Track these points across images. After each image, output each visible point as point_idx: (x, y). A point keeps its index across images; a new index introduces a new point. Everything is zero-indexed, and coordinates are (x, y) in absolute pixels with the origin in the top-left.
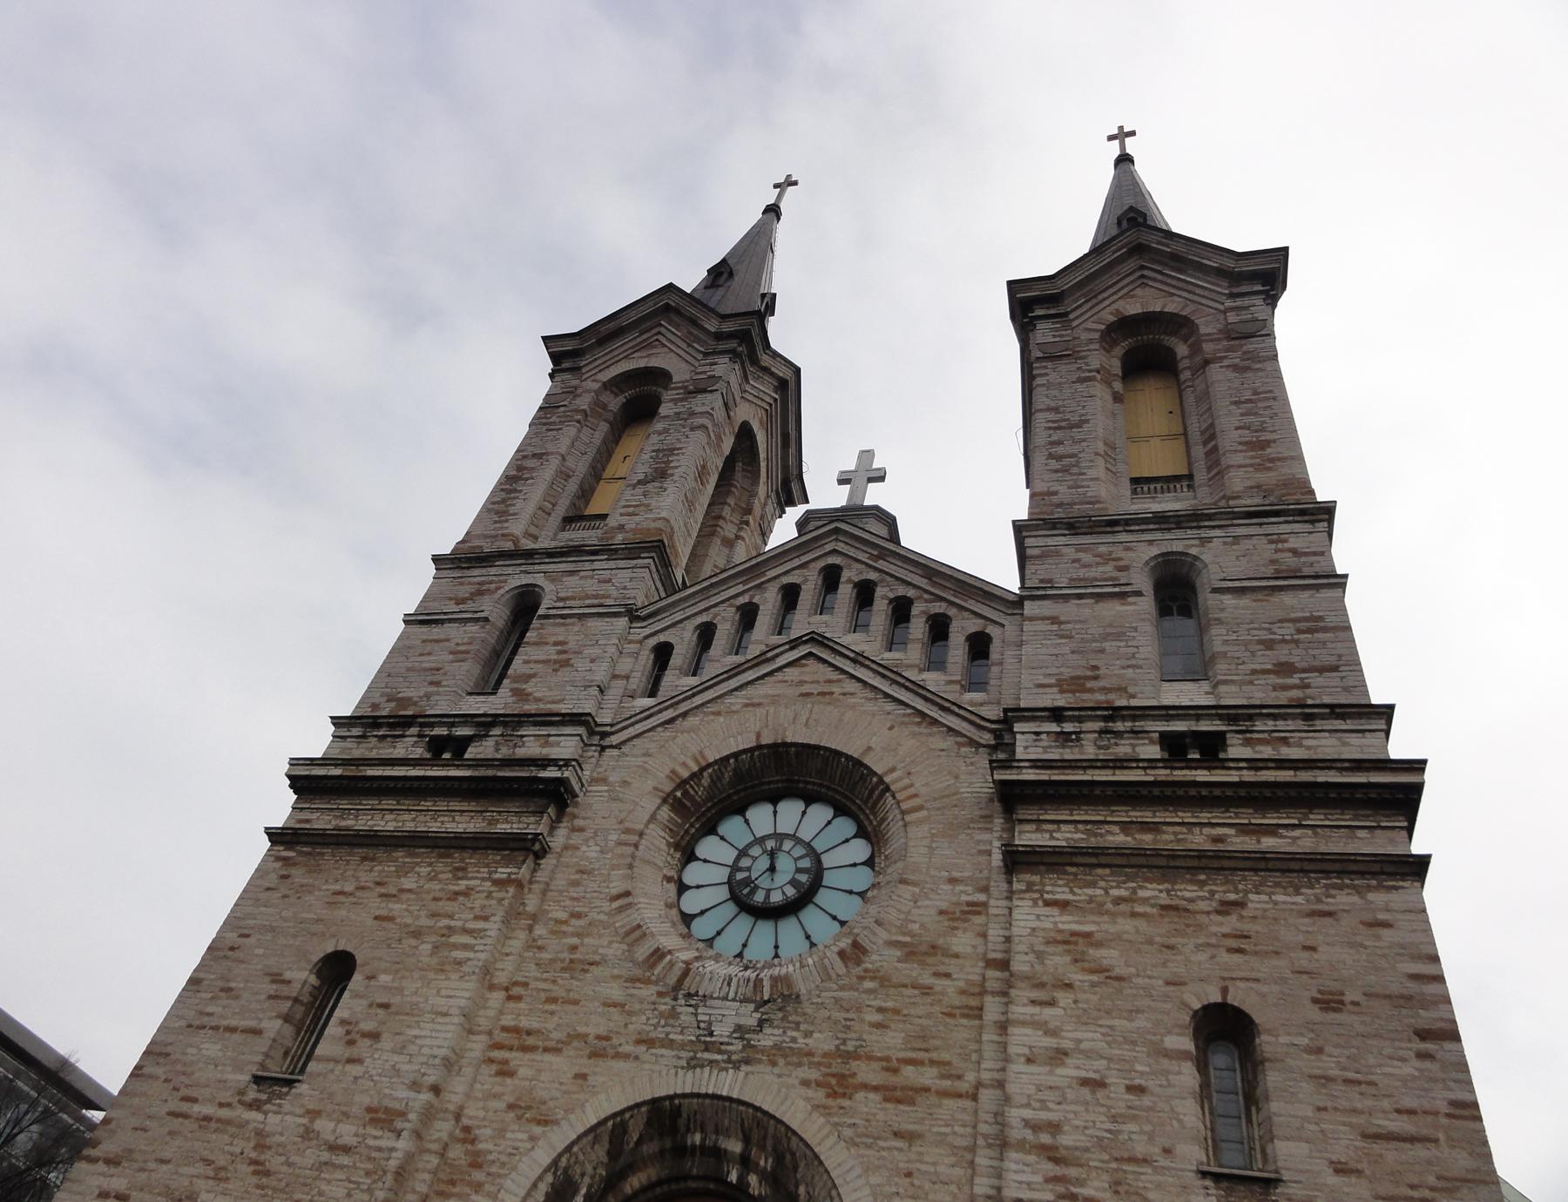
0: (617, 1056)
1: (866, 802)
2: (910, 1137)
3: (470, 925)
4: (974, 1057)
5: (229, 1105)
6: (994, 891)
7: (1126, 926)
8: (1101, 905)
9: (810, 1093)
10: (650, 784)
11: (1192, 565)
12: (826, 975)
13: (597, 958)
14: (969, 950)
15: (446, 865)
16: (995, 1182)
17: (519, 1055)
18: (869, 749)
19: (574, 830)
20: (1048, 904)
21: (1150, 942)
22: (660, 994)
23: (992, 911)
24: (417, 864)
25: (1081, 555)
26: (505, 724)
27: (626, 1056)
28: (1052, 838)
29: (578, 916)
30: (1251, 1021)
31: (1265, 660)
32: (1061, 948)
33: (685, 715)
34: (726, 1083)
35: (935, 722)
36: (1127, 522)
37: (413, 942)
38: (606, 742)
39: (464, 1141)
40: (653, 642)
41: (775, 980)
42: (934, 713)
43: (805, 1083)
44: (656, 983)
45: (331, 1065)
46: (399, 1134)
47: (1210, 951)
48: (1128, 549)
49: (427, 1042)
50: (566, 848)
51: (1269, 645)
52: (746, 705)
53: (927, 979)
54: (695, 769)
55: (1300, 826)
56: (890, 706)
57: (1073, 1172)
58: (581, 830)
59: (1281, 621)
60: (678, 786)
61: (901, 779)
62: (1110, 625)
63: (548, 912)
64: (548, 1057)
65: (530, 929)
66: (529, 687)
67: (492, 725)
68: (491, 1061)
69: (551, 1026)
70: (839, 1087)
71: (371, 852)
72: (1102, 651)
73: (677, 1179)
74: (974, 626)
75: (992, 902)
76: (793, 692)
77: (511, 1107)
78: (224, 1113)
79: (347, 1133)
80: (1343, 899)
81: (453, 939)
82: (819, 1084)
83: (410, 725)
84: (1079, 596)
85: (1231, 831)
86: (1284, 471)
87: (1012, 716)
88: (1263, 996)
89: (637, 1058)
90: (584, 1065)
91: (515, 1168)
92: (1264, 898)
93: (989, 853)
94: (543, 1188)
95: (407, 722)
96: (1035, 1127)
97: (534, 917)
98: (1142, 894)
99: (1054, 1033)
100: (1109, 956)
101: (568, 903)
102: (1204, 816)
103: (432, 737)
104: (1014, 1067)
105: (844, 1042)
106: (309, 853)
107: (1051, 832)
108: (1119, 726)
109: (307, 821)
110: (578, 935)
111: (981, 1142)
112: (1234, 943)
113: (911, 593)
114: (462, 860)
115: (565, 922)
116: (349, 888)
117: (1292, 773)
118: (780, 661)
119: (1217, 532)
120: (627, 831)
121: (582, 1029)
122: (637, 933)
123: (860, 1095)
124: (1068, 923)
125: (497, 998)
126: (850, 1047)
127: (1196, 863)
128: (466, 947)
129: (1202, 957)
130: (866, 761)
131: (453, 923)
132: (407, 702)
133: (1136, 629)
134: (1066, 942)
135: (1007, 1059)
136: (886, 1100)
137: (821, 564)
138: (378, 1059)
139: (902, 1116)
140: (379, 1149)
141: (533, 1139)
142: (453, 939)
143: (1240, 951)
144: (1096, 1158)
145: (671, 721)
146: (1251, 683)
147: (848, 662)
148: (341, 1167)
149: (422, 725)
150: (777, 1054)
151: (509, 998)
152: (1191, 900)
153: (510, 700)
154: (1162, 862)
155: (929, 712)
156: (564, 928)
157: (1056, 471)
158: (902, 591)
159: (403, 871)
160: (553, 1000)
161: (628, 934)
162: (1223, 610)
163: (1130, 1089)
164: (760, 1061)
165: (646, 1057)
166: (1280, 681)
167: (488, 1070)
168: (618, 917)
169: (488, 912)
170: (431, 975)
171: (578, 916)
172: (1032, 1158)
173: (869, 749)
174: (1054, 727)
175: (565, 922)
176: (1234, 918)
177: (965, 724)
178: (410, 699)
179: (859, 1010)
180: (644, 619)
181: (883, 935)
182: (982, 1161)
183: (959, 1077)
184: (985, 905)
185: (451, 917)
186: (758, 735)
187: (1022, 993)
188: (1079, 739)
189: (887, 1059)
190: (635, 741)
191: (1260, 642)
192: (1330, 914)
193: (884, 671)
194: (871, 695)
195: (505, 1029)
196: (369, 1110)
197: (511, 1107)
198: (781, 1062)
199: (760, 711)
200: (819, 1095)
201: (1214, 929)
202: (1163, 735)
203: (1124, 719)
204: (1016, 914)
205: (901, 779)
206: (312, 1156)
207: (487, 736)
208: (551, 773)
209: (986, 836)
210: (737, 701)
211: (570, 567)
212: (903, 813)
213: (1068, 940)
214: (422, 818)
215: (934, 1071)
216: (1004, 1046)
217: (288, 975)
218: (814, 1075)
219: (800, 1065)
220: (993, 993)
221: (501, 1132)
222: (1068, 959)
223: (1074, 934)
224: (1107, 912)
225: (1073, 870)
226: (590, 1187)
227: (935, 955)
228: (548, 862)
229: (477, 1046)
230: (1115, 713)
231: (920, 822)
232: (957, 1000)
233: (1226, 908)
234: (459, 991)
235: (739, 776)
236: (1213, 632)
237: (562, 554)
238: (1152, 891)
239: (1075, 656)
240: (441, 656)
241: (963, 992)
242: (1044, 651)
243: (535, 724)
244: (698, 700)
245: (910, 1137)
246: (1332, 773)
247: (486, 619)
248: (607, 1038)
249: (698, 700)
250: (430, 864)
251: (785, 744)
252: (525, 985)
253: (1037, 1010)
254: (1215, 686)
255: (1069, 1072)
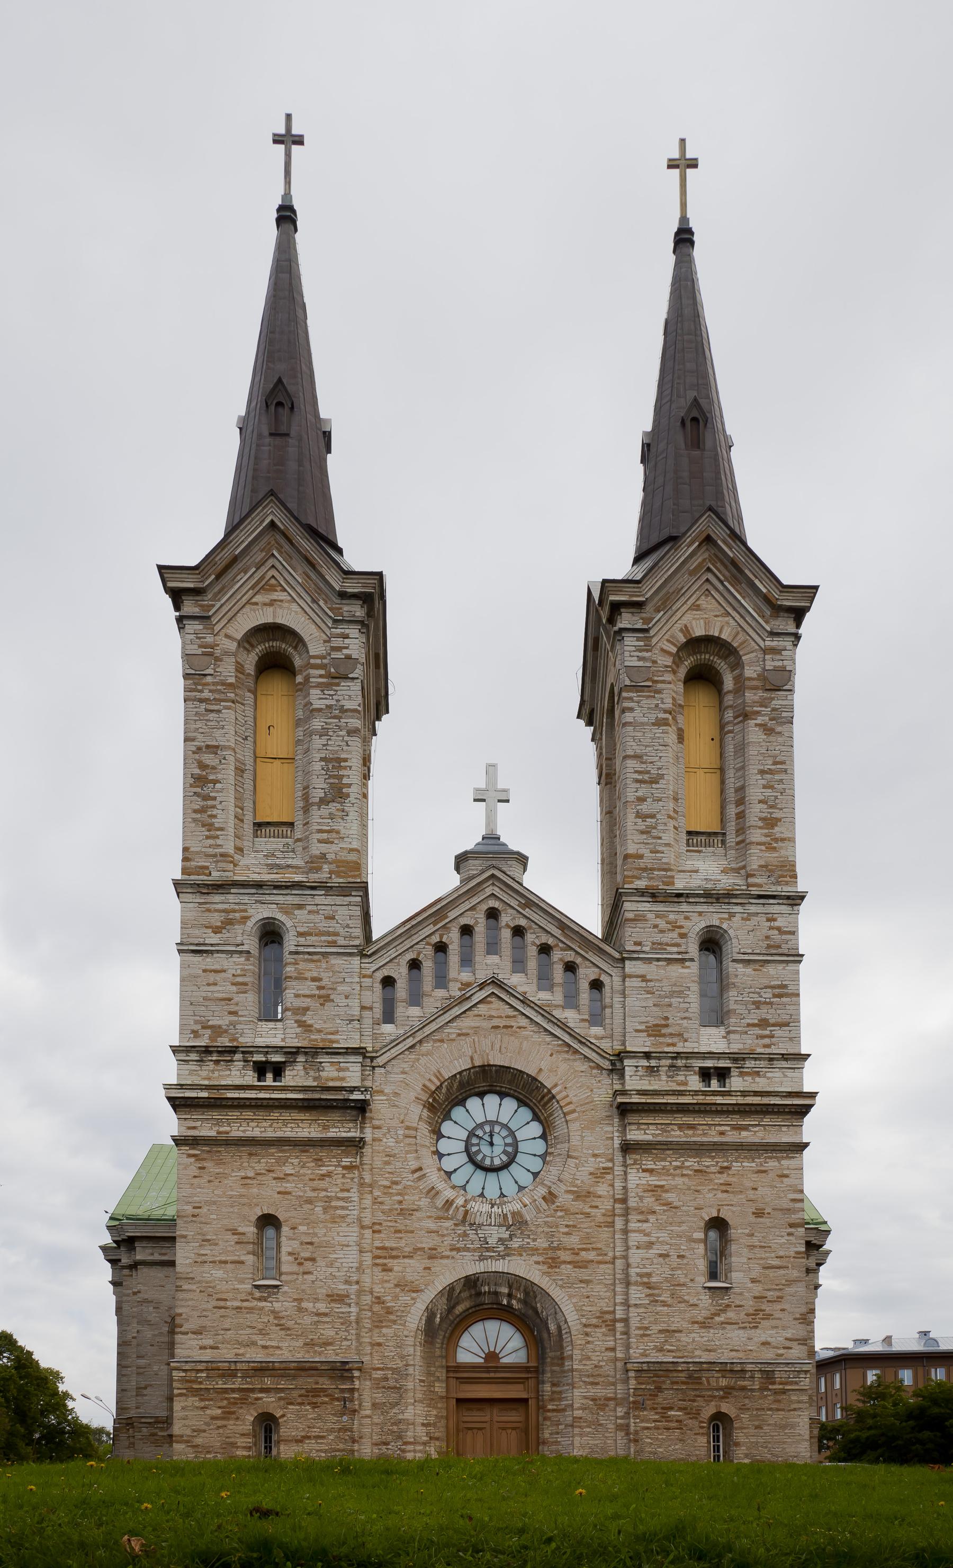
0: (442, 1257)
1: (539, 1102)
2: (587, 1282)
3: (340, 1195)
4: (612, 1245)
5: (247, 1300)
6: (617, 1163)
7: (679, 1181)
8: (668, 1170)
9: (540, 1267)
10: (412, 1095)
11: (722, 935)
12: (538, 1210)
13: (415, 1207)
14: (606, 1193)
15: (308, 1157)
16: (624, 1297)
17: (391, 1260)
18: (541, 1070)
19: (374, 1128)
20: (644, 1171)
21: (689, 1189)
22: (455, 1225)
23: (616, 1173)
24: (288, 1157)
25: (658, 921)
26: (306, 1053)
27: (448, 1257)
28: (645, 1133)
29: (396, 1183)
30: (728, 1223)
31: (753, 1018)
32: (651, 1193)
33: (420, 1042)
34: (500, 1266)
35: (576, 1052)
36: (688, 895)
37: (309, 1206)
38: (373, 1064)
39: (379, 1303)
40: (379, 975)
41: (514, 1214)
42: (576, 1046)
43: (537, 1263)
44: (451, 1219)
45: (295, 1276)
46: (350, 1305)
47: (715, 1192)
48: (687, 918)
49: (344, 1260)
50: (373, 1140)
51: (758, 1005)
52: (459, 1035)
53: (589, 1210)
54: (439, 1084)
55: (759, 1125)
56: (549, 1039)
57: (656, 1292)
58: (379, 1128)
59: (766, 987)
60: (431, 1096)
61: (560, 1092)
62: (675, 985)
63: (377, 1181)
64: (406, 1261)
65: (371, 1192)
66: (308, 1018)
67: (297, 1053)
68: (377, 1265)
69: (402, 1244)
70: (553, 1263)
71: (253, 1149)
72: (670, 1005)
73: (478, 1305)
74: (592, 974)
75: (616, 1168)
76: (487, 1024)
77: (396, 1286)
78: (245, 1304)
79: (322, 1307)
80: (772, 1164)
81: (333, 1204)
82: (544, 1263)
83: (234, 1052)
84: (658, 960)
85: (728, 1128)
86: (783, 852)
87: (621, 1056)
88: (733, 1212)
89: (453, 1258)
90: (427, 1263)
91: (409, 1312)
92: (739, 1164)
93: (612, 1138)
94: (424, 1318)
95: (233, 1051)
96: (641, 1275)
97: (371, 1186)
98: (687, 1164)
99: (646, 1235)
100: (671, 1197)
101: (387, 1175)
102: (717, 1120)
103: (254, 1062)
104: (631, 1251)
105: (552, 1242)
106: (209, 1152)
107: (645, 1130)
108: (680, 1063)
109: (194, 1128)
110: (400, 1194)
111: (617, 1282)
112: (724, 1188)
113: (551, 941)
114: (317, 1154)
115: (390, 1187)
116: (251, 1174)
117: (759, 1098)
118: (476, 999)
119: (738, 909)
120: (408, 1128)
121: (419, 1245)
122: (433, 1192)
123: (563, 1266)
124: (654, 1180)
125: (368, 1233)
126: (555, 1244)
127: (711, 1147)
128: (343, 1208)
129: (711, 1195)
131: (329, 1194)
132: (217, 1031)
133: (689, 988)
134: (653, 1191)
135: (628, 1248)
136: (575, 1267)
137: (484, 907)
138: (321, 1271)
139: (584, 1274)
140: (343, 1313)
141: (413, 1299)
142: (333, 1204)
143: (727, 1191)
144: (665, 1285)
145: (413, 1047)
146: (746, 1033)
147: (519, 1002)
148: (327, 1322)
149: (243, 1052)
150: (521, 1250)
151: (374, 1232)
152: (708, 1167)
153: (299, 1030)
154: (697, 1147)
155: (573, 1044)
156: (391, 1191)
157: (642, 832)
158: (545, 939)
159: (282, 1162)
160: (400, 1231)
162: (736, 976)
163: (679, 1257)
164: (514, 1255)
165: (458, 1256)
166: (760, 1032)
167: (376, 1269)
168: (420, 1183)
169: (347, 1187)
170: (330, 1225)
171: (396, 1183)
172: (640, 1288)
173: (541, 1070)
174: (644, 1063)
175: (390, 1187)
176: (725, 1175)
177: (594, 1054)
178: (220, 1027)
179: (557, 1226)
180: (370, 956)
181: (564, 1188)
182: (619, 1289)
183: (606, 1255)
184: (612, 1169)
185: (326, 1190)
186: (472, 1059)
187: (633, 1217)
188: (658, 1071)
189: (573, 1249)
190: (393, 1062)
191: (754, 1003)
192: (765, 1172)
193: (540, 1009)
194: (535, 1029)
195: (378, 1248)
196: (328, 1296)
197: (396, 1286)
198: (524, 1254)
199: (468, 1039)
200: (544, 1268)
201: (716, 1181)
202: (700, 1068)
203: (682, 1058)
204: (629, 1177)
205: (560, 1092)
206: (308, 1320)
207: (295, 1062)
208: (356, 1096)
209: (610, 1129)
210: (452, 1030)
211: (296, 900)
212: (565, 1114)
213: (655, 1190)
214: (275, 1125)
215: (594, 1253)
216: (626, 1240)
217: (241, 1230)
218: (541, 1259)
219: (533, 1255)
220: (619, 1216)
221: (396, 1298)
222: (653, 1199)
223: (656, 1186)
224: (671, 1175)
225: (655, 1151)
226: (441, 1314)
227: (589, 1197)
228: (367, 1150)
229: (368, 1259)
230: (678, 1056)
231: (575, 1120)
232: (602, 1219)
233: (724, 1170)
234: (351, 1234)
235: (462, 1085)
236: (731, 994)
237: (287, 887)
238: (691, 1162)
239: (655, 1009)
240: (225, 989)
241: (604, 1215)
242: (637, 1003)
243: (327, 1053)
244: (427, 1030)
245: (587, 1282)
246: (777, 1098)
247: (248, 952)
248: (435, 1249)
249: (427, 1030)
250: (297, 1157)
251: (489, 1065)
252: (380, 1224)
253: (640, 1224)
254: (728, 1033)
255: (654, 1251)
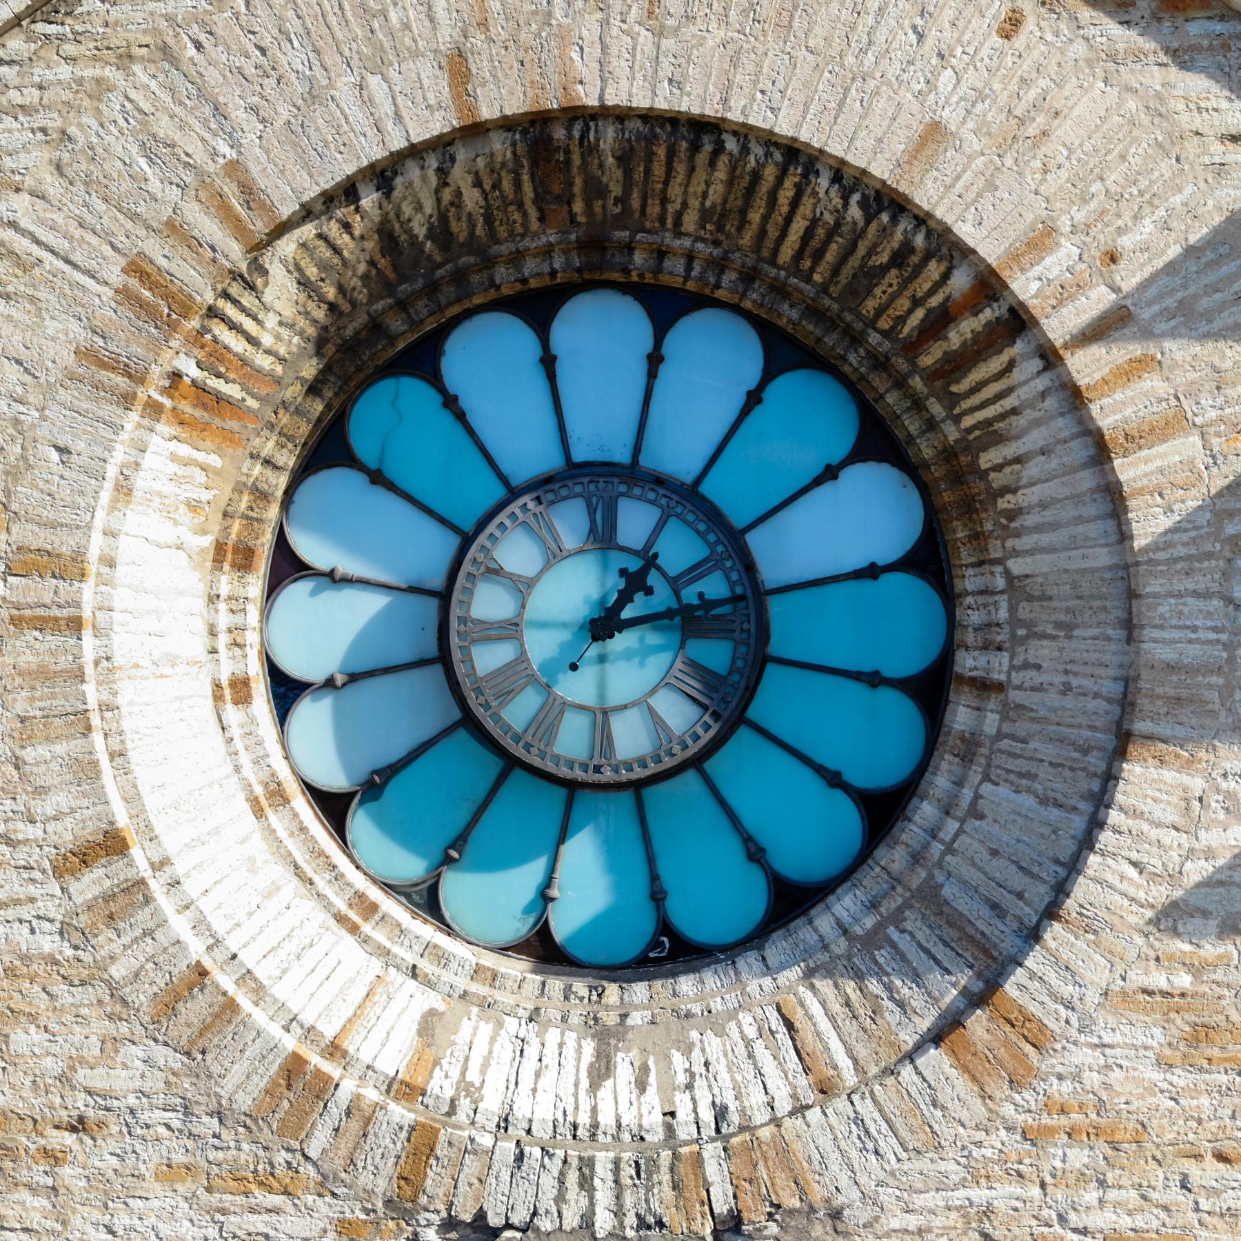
1: (913, 347)
122: (196, 1009)
130: (927, 194)
161: (169, 1003)
168: (108, 943)
181: (1097, 973)
186: (458, 68)
